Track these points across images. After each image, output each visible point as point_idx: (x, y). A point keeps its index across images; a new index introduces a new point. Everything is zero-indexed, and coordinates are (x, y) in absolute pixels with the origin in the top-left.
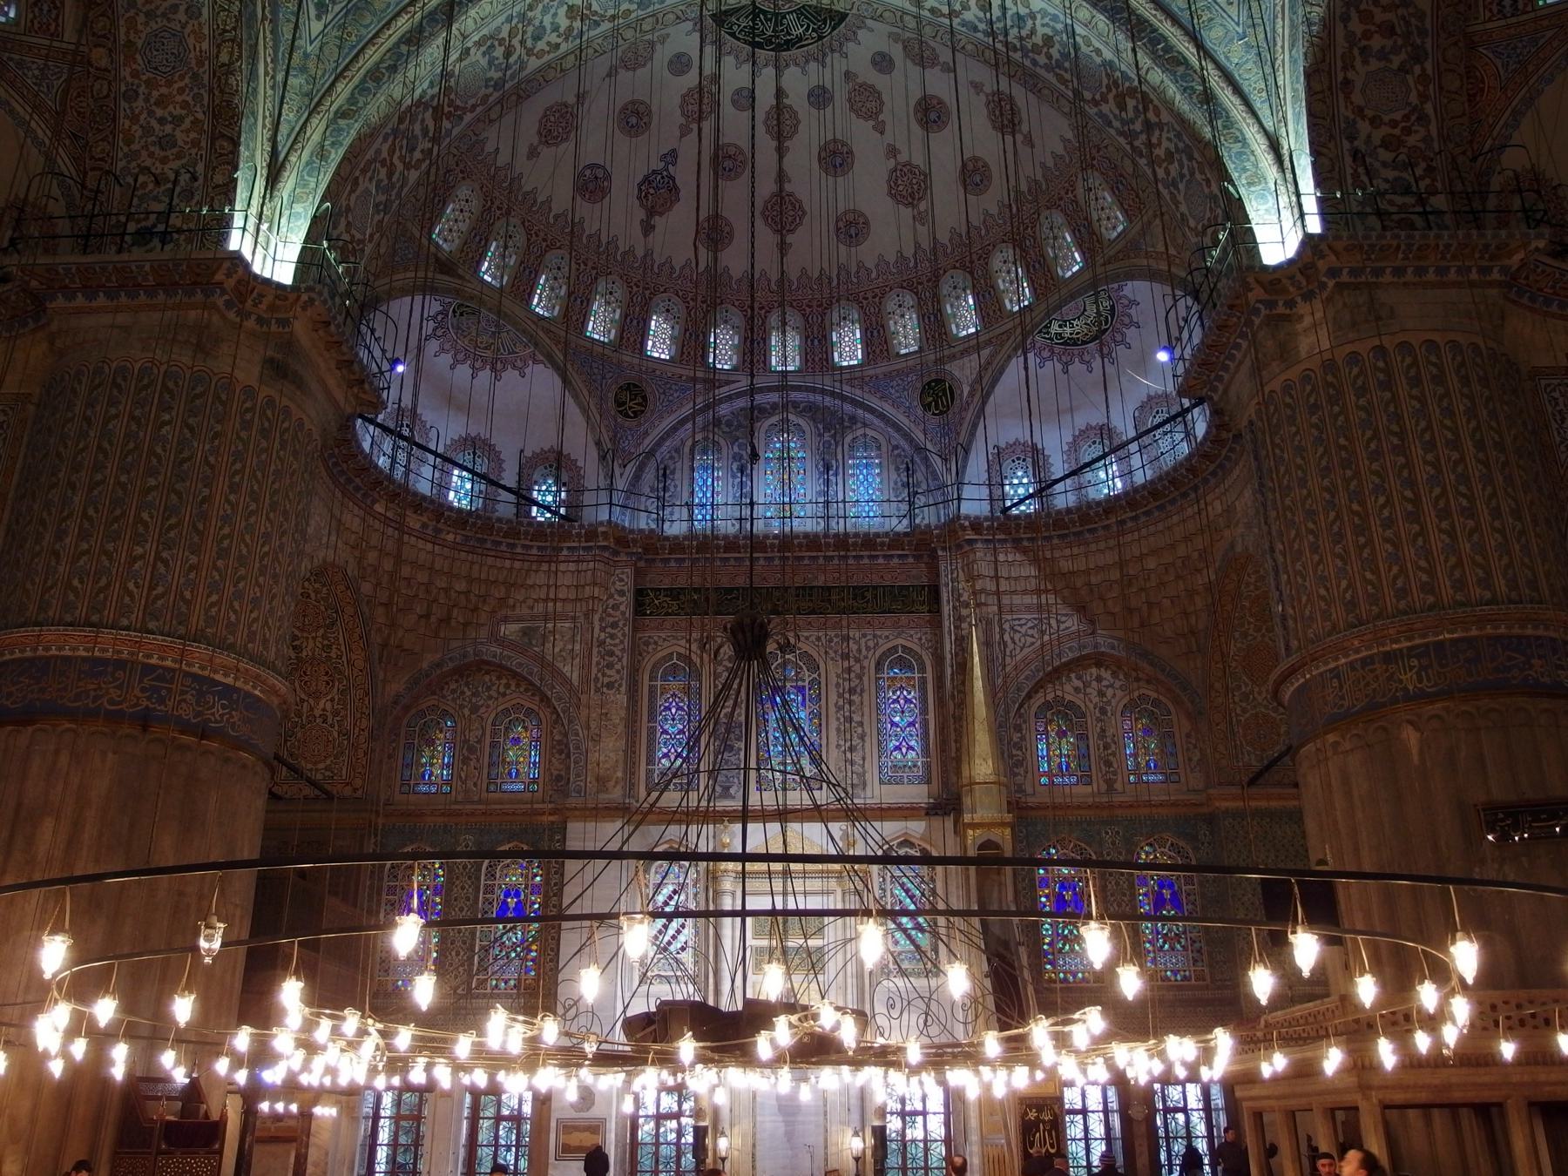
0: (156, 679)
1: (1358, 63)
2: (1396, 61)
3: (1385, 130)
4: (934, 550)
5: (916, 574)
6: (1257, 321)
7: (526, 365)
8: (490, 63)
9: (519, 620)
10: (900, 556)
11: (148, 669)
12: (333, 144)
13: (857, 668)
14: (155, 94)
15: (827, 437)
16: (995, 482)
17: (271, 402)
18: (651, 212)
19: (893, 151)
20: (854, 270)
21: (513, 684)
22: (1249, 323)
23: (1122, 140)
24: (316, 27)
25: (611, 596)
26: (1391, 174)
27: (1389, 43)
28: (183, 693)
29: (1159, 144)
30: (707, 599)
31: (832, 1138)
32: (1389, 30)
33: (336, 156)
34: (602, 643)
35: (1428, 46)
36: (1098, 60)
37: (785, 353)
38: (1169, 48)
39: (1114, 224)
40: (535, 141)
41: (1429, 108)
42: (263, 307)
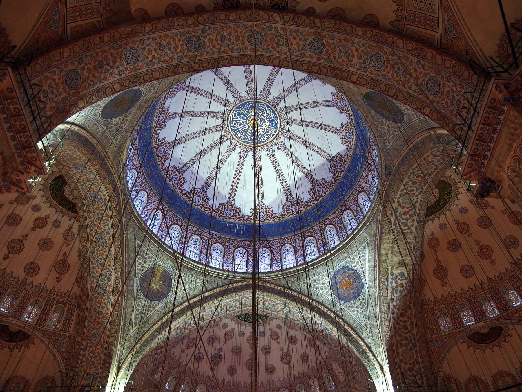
1: (400, 347)
2: (409, 347)
3: (408, 366)
8: (176, 334)
14: (91, 349)
19: (282, 349)
20: (271, 382)
24: (134, 329)
26: (411, 378)
27: (407, 342)
32: (406, 339)
33: (134, 365)
35: (417, 343)
38: (353, 338)
40: (184, 347)
41: (419, 359)
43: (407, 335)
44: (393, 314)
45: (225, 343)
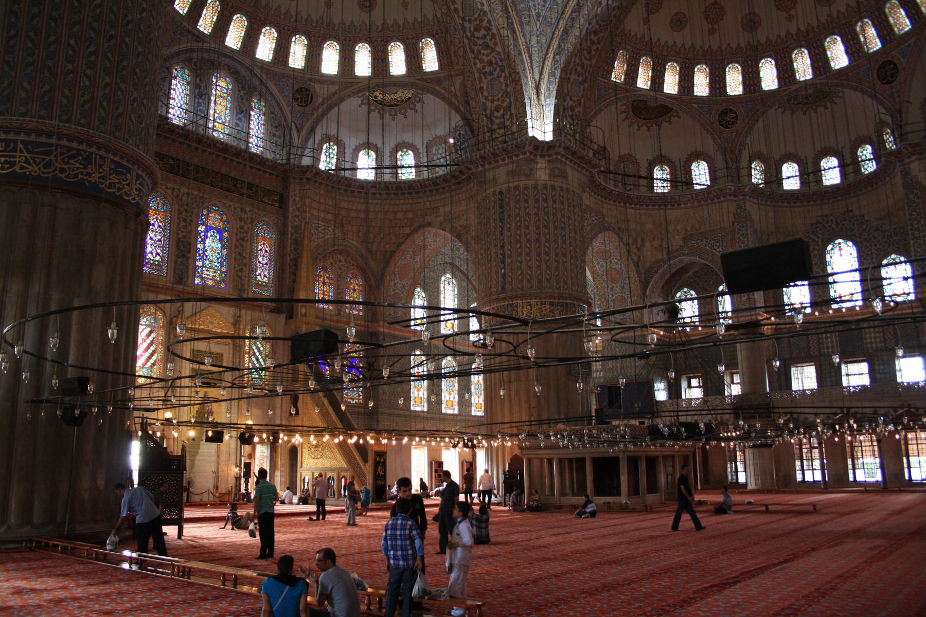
6: (521, 156)
10: (271, 174)
13: (246, 227)
15: (242, 93)
22: (517, 155)
23: (466, 41)
29: (487, 55)
30: (178, 166)
31: (223, 468)
36: (480, 7)
43: (586, 62)
44: (590, 24)
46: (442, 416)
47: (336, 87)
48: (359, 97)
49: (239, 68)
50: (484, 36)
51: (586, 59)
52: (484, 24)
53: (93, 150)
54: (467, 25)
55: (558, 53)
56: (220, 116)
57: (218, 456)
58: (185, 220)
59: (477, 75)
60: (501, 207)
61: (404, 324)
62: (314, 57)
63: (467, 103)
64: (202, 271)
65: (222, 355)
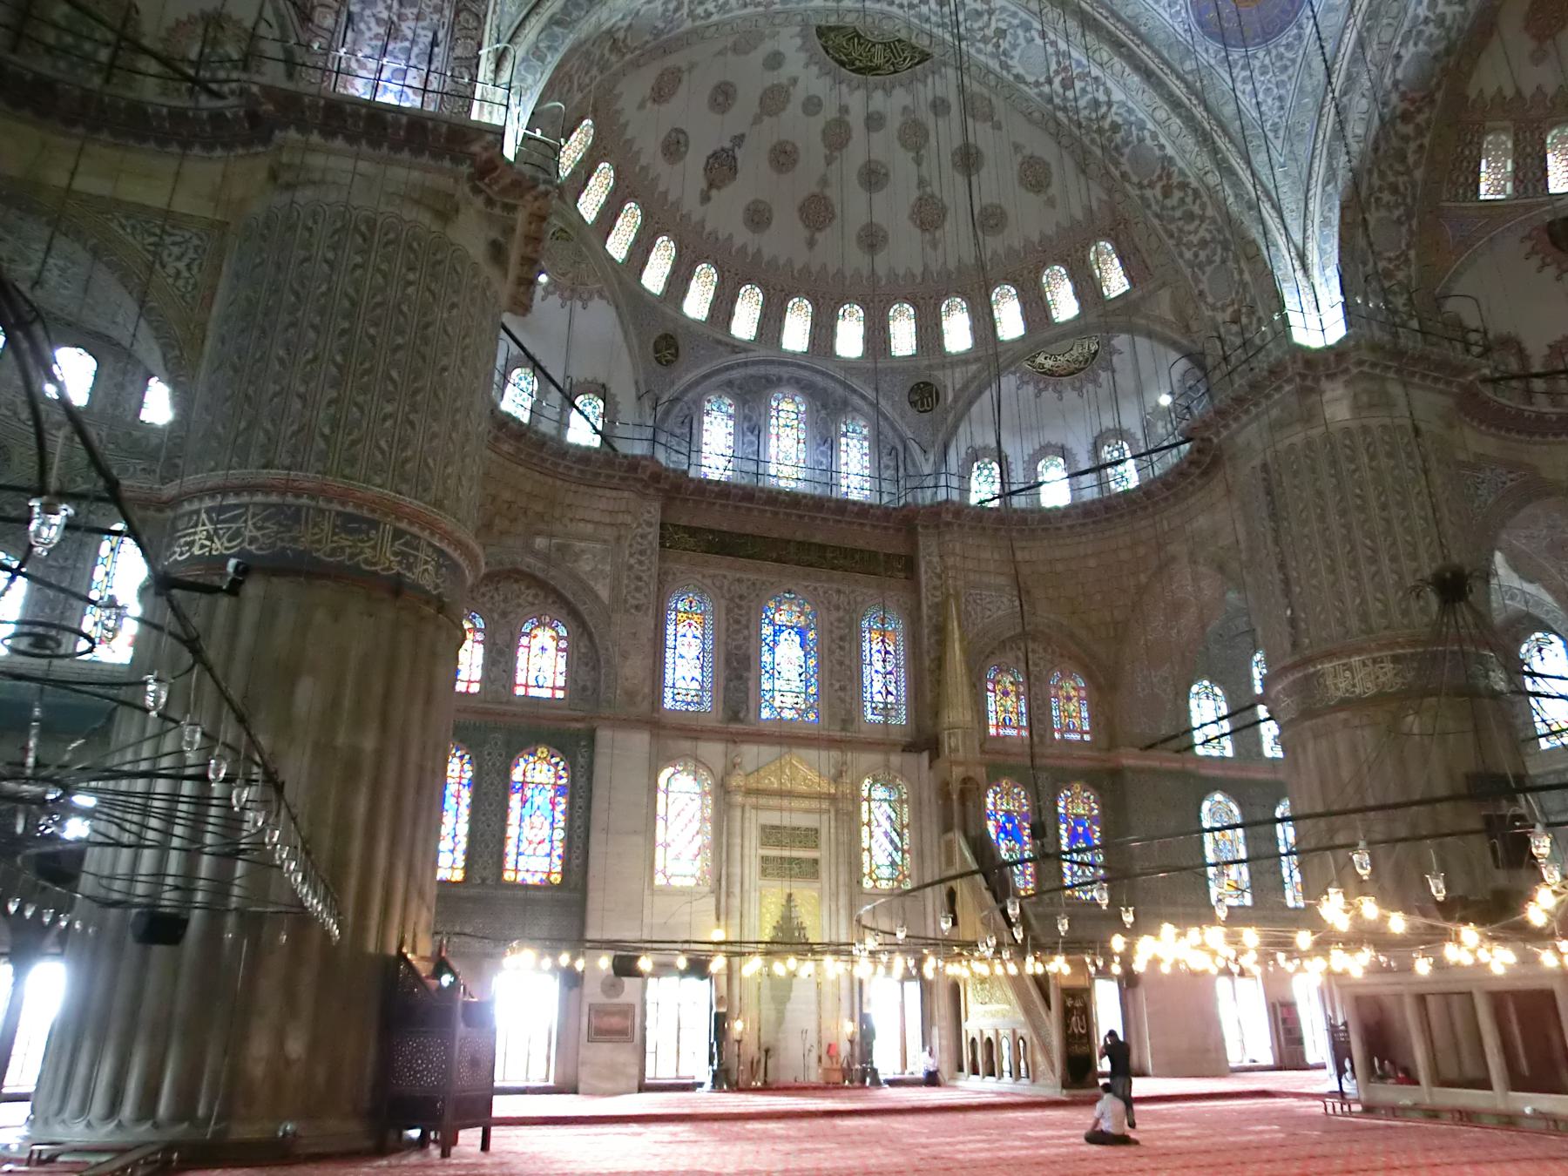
0: (405, 544)
2: (1397, 213)
4: (915, 528)
5: (896, 546)
7: (591, 297)
9: (551, 536)
10: (886, 528)
11: (398, 534)
12: (549, 48)
15: (823, 413)
16: (965, 477)
17: (489, 283)
18: (711, 185)
19: (922, 183)
21: (542, 594)
23: (1156, 222)
25: (639, 525)
27: (1393, 199)
28: (426, 562)
29: (1196, 232)
31: (828, 1022)
32: (1394, 189)
33: (553, 60)
34: (631, 567)
37: (796, 334)
38: (1225, 160)
39: (1115, 282)
42: (496, 188)
45: (757, 120)
46: (1287, 914)
47: (974, 367)
48: (1014, 373)
49: (818, 379)
50: (1182, 200)
51: (1398, 173)
52: (1175, 180)
53: (304, 501)
54: (1148, 193)
55: (1331, 176)
56: (787, 457)
57: (819, 1003)
58: (738, 622)
59: (1188, 272)
60: (1269, 493)
61: (1174, 744)
62: (929, 332)
63: (1187, 328)
64: (773, 697)
65: (816, 831)
